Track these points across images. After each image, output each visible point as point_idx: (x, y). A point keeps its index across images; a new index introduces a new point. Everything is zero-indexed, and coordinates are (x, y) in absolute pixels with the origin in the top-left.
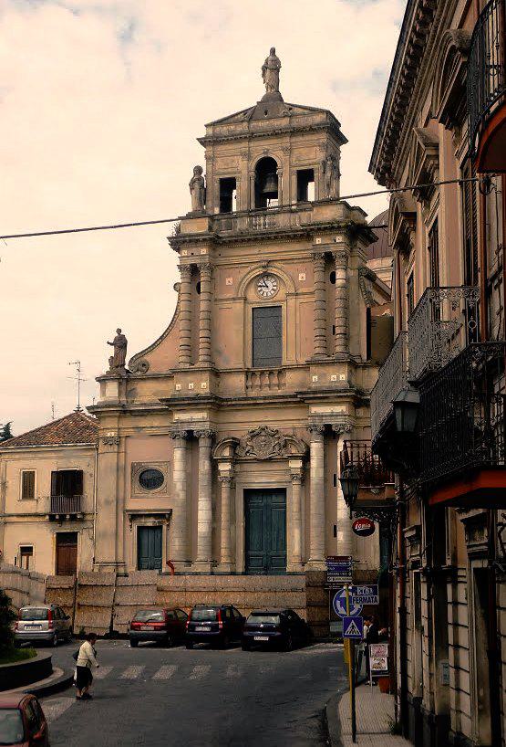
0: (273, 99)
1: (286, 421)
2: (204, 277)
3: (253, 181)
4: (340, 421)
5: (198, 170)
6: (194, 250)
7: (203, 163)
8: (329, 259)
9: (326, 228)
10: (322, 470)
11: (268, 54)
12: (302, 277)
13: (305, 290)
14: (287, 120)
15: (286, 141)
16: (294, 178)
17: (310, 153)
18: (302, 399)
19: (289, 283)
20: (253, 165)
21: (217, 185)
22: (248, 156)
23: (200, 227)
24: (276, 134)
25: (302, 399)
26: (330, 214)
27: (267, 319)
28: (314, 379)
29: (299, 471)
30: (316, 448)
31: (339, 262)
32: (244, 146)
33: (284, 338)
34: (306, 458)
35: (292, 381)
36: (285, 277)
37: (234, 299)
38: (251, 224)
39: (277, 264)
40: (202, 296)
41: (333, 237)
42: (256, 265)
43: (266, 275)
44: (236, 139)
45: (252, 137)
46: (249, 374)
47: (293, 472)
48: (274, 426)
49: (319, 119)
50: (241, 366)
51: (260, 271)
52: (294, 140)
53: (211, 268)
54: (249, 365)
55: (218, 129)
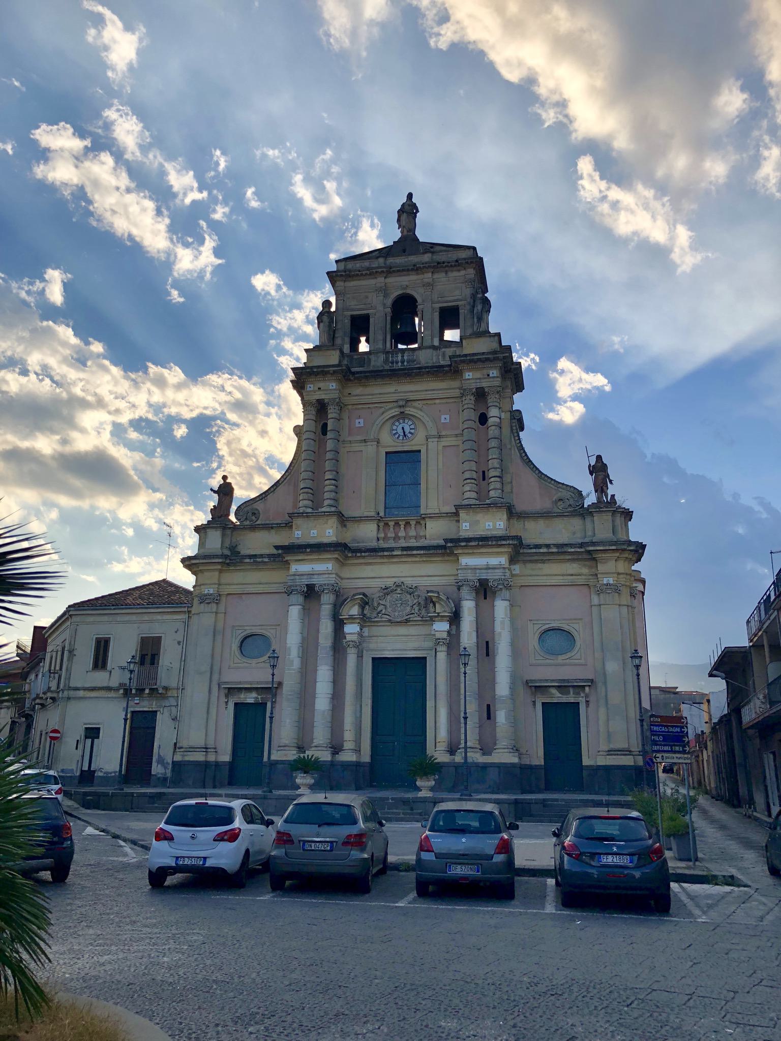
0: (408, 243)
1: (428, 575)
2: (332, 413)
3: (389, 318)
4: (497, 575)
5: (327, 304)
6: (321, 385)
7: (333, 300)
8: (481, 395)
9: (480, 360)
10: (474, 634)
11: (404, 199)
12: (445, 418)
13: (448, 433)
14: (429, 255)
15: (428, 276)
16: (436, 316)
17: (452, 288)
18: (448, 548)
19: (430, 424)
20: (389, 302)
21: (347, 322)
22: (385, 291)
23: (333, 358)
24: (416, 269)
25: (448, 548)
26: (480, 346)
27: (403, 463)
28: (467, 527)
29: (445, 635)
30: (468, 606)
31: (491, 399)
32: (381, 280)
33: (423, 486)
34: (455, 618)
35: (435, 531)
36: (426, 419)
37: (365, 441)
38: (386, 361)
39: (416, 404)
40: (330, 435)
41: (485, 372)
42: (391, 405)
43: (403, 416)
44: (372, 273)
45: (389, 271)
46: (381, 521)
47: (438, 635)
48: (409, 581)
49: (463, 254)
50: (373, 514)
51: (395, 412)
52: (436, 276)
53: (341, 406)
54: (382, 514)
55: (350, 265)
